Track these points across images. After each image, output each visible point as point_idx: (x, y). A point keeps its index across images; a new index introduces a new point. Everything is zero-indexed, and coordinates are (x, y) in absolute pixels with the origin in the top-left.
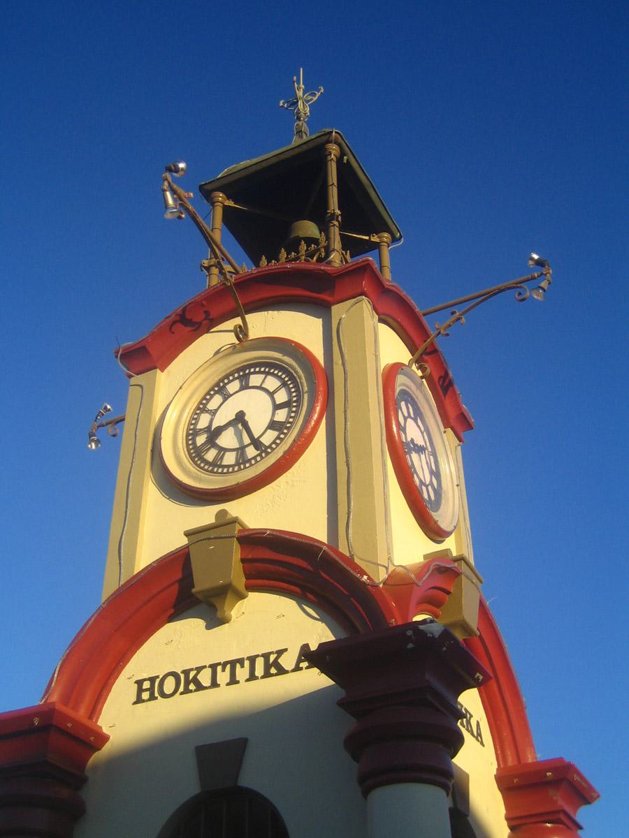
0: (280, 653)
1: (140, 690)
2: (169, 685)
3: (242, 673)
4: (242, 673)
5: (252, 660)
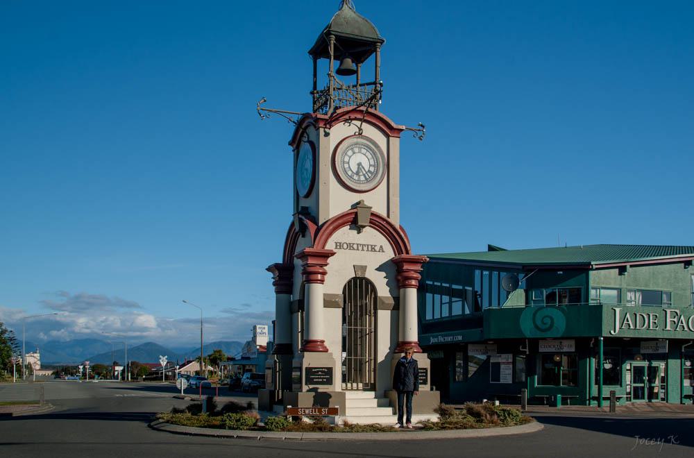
0: (375, 246)
1: (336, 246)
2: (345, 246)
3: (365, 248)
4: (365, 248)
5: (368, 245)
